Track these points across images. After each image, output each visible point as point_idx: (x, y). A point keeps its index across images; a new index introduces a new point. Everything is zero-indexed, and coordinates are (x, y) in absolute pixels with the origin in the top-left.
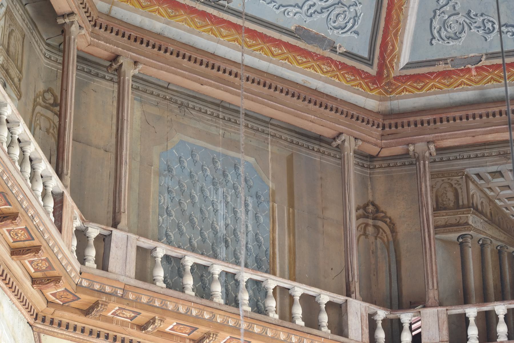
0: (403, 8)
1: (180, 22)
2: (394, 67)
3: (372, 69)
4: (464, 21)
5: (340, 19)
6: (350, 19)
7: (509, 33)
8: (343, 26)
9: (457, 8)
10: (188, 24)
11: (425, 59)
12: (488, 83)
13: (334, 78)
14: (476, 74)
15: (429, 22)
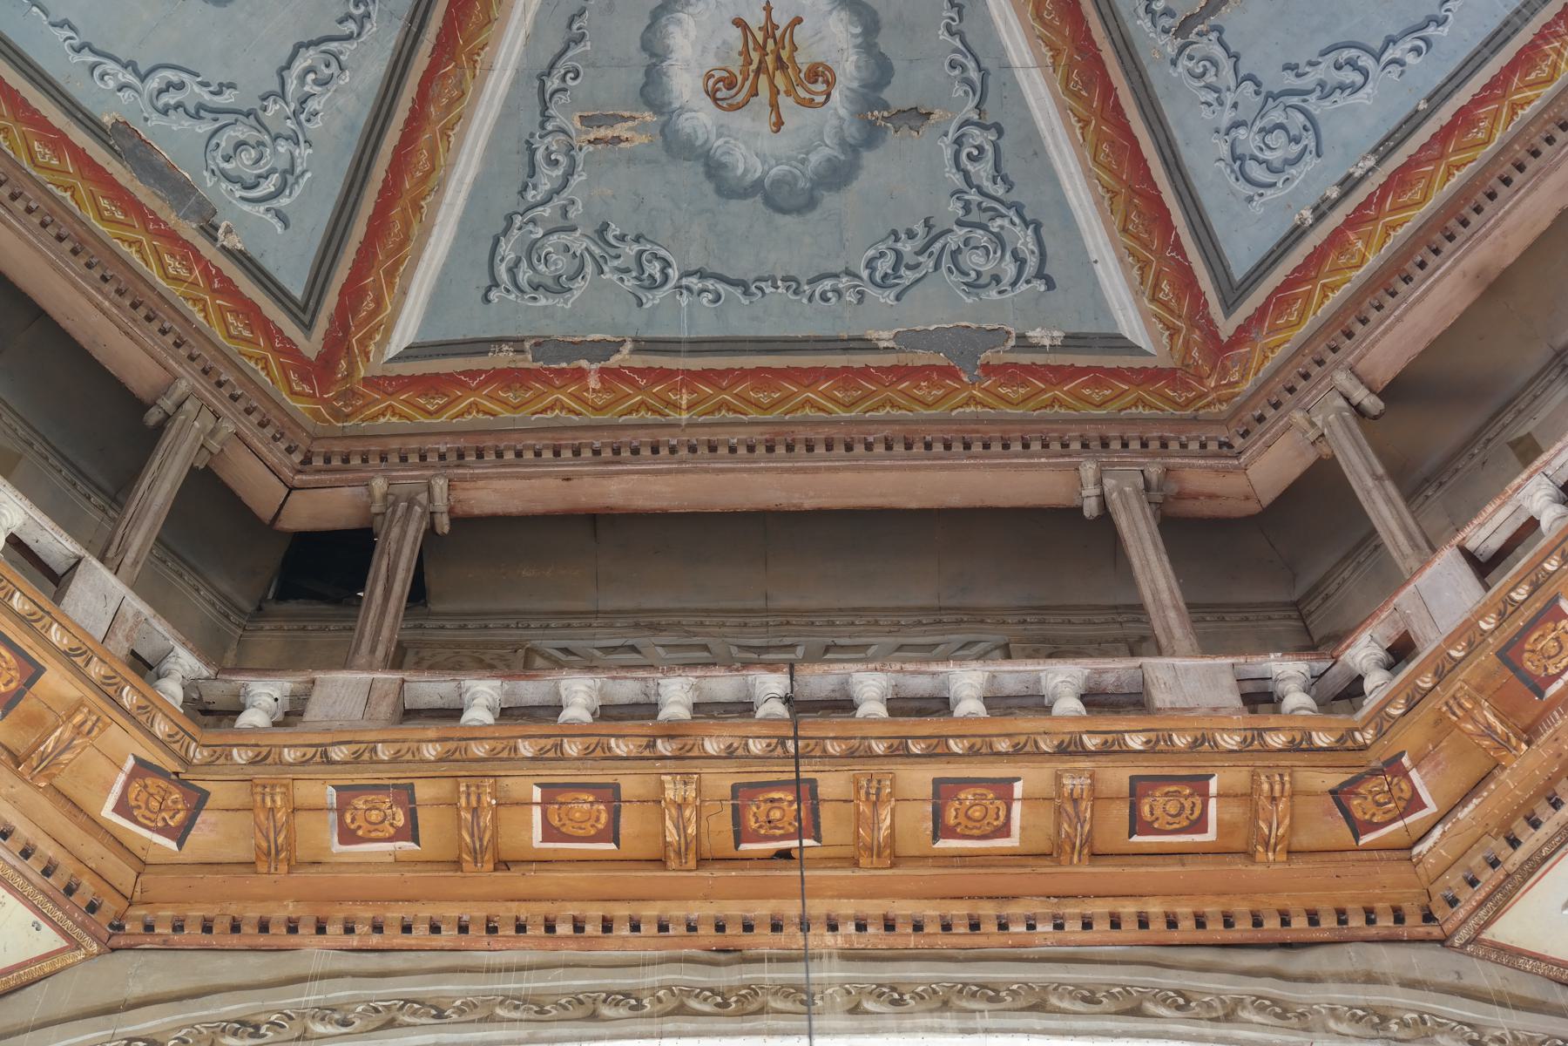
0: (423, 203)
2: (371, 356)
3: (308, 338)
4: (587, 249)
5: (247, 157)
6: (273, 171)
7: (705, 294)
8: (250, 181)
9: (572, 214)
11: (460, 337)
12: (630, 413)
13: (195, 305)
14: (598, 387)
15: (490, 242)
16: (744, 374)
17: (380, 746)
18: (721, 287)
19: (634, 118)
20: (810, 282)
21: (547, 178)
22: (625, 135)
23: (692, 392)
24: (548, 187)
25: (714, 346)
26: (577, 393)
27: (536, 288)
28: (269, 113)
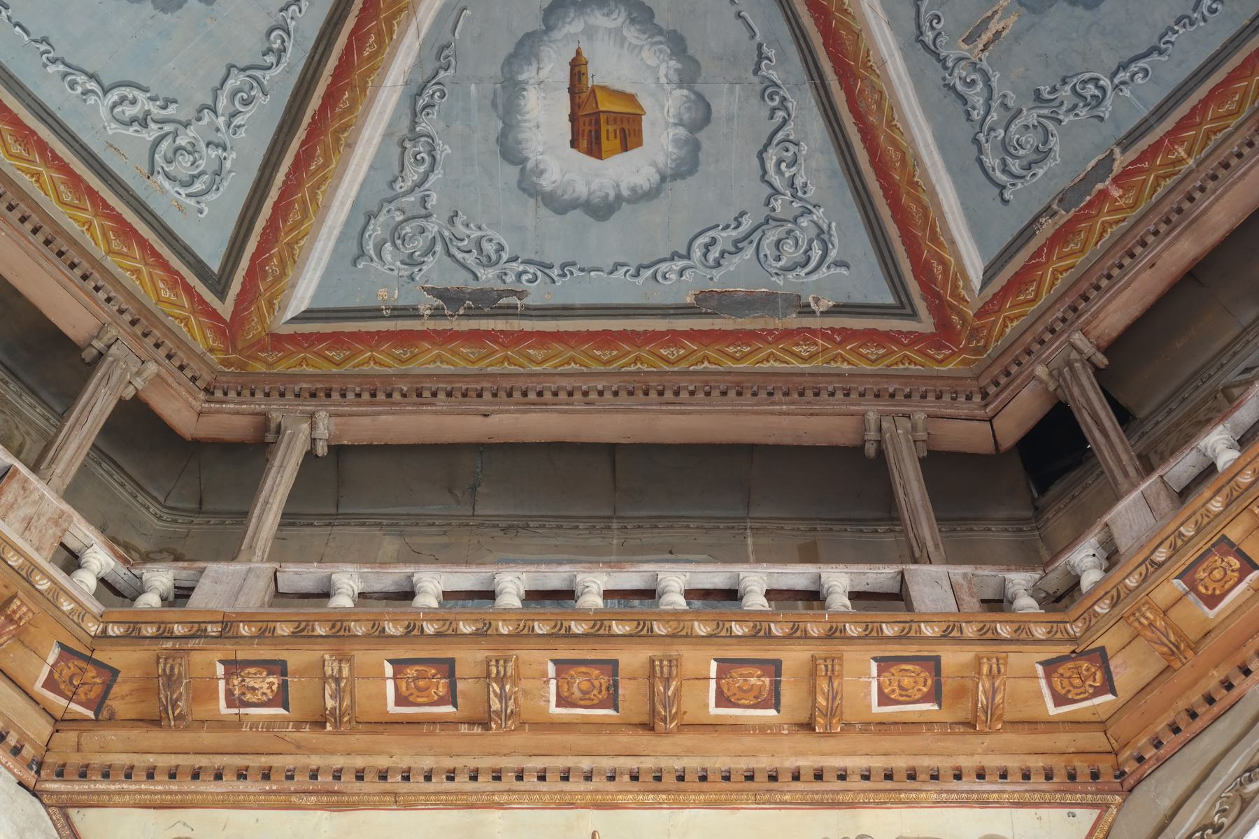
0: (916, 179)
1: (429, 363)
2: (967, 297)
3: (920, 321)
4: (1038, 116)
5: (788, 247)
7: (1136, 77)
8: (803, 259)
9: (1011, 103)
10: (448, 363)
11: (1010, 239)
12: (1155, 191)
13: (836, 362)
14: (1121, 192)
16: (1205, 103)
17: (1182, 529)
18: (1142, 64)
19: (996, 12)
20: (1195, 10)
21: (976, 97)
22: (1000, 27)
23: (1182, 143)
24: (981, 101)
25: (1170, 103)
26: (1111, 208)
27: (1029, 167)
28: (778, 210)
